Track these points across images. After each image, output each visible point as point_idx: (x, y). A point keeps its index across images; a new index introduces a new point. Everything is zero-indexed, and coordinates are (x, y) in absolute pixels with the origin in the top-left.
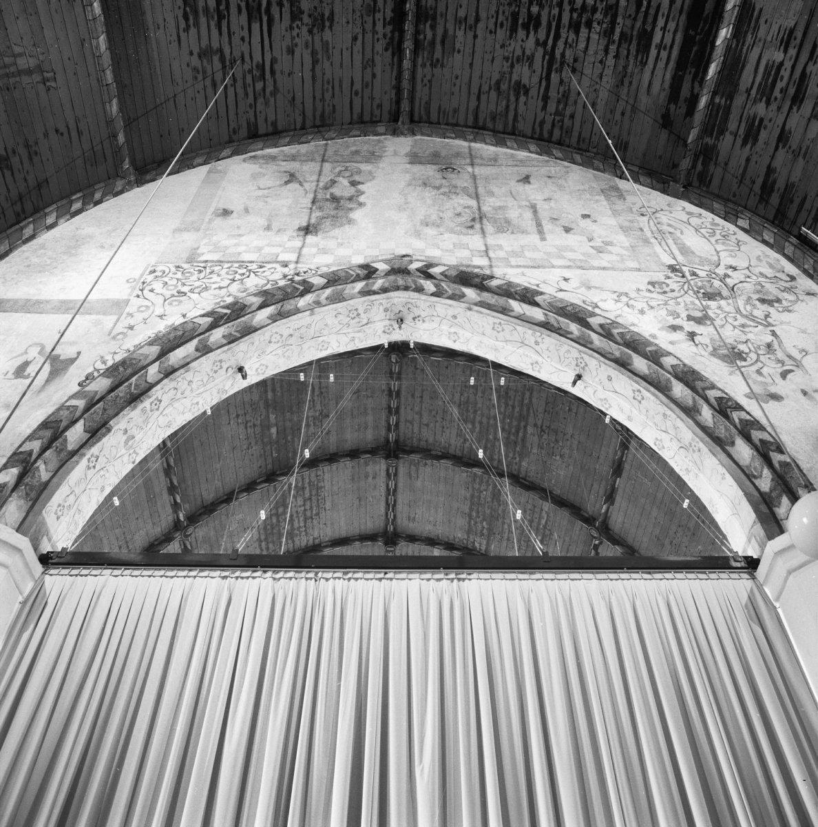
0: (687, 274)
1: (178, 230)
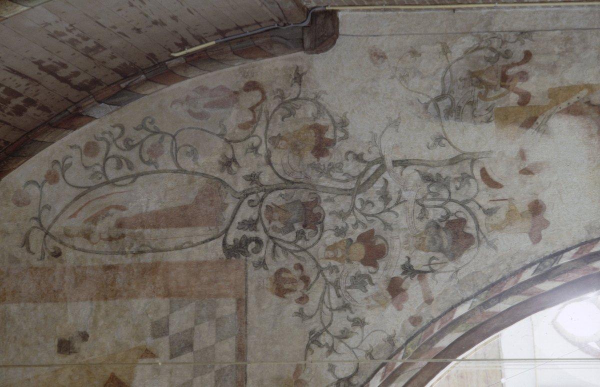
0: (251, 234)
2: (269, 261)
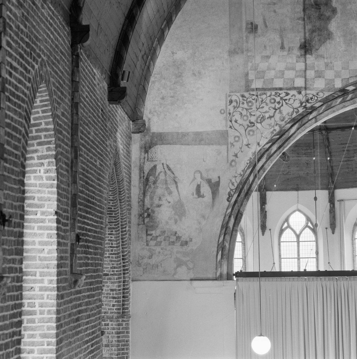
1: (232, 53)
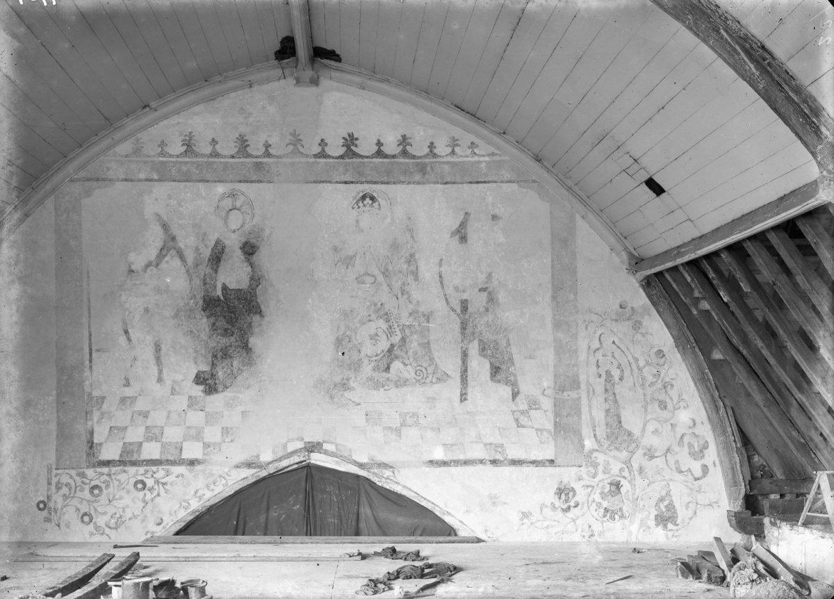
0: (601, 468)
2: (582, 483)
